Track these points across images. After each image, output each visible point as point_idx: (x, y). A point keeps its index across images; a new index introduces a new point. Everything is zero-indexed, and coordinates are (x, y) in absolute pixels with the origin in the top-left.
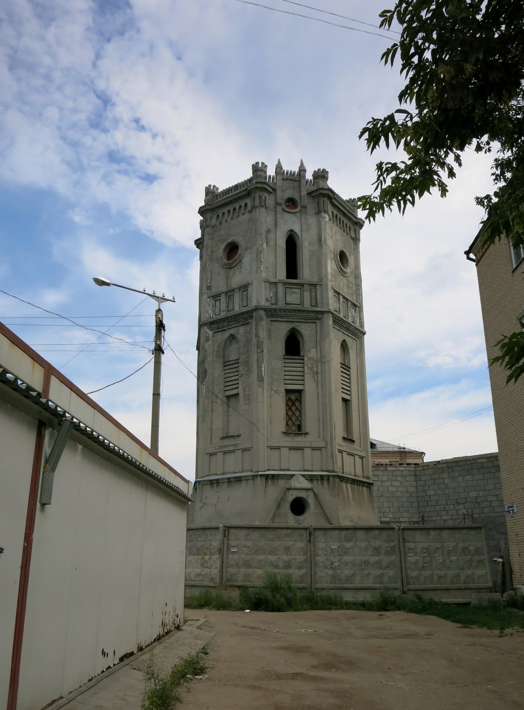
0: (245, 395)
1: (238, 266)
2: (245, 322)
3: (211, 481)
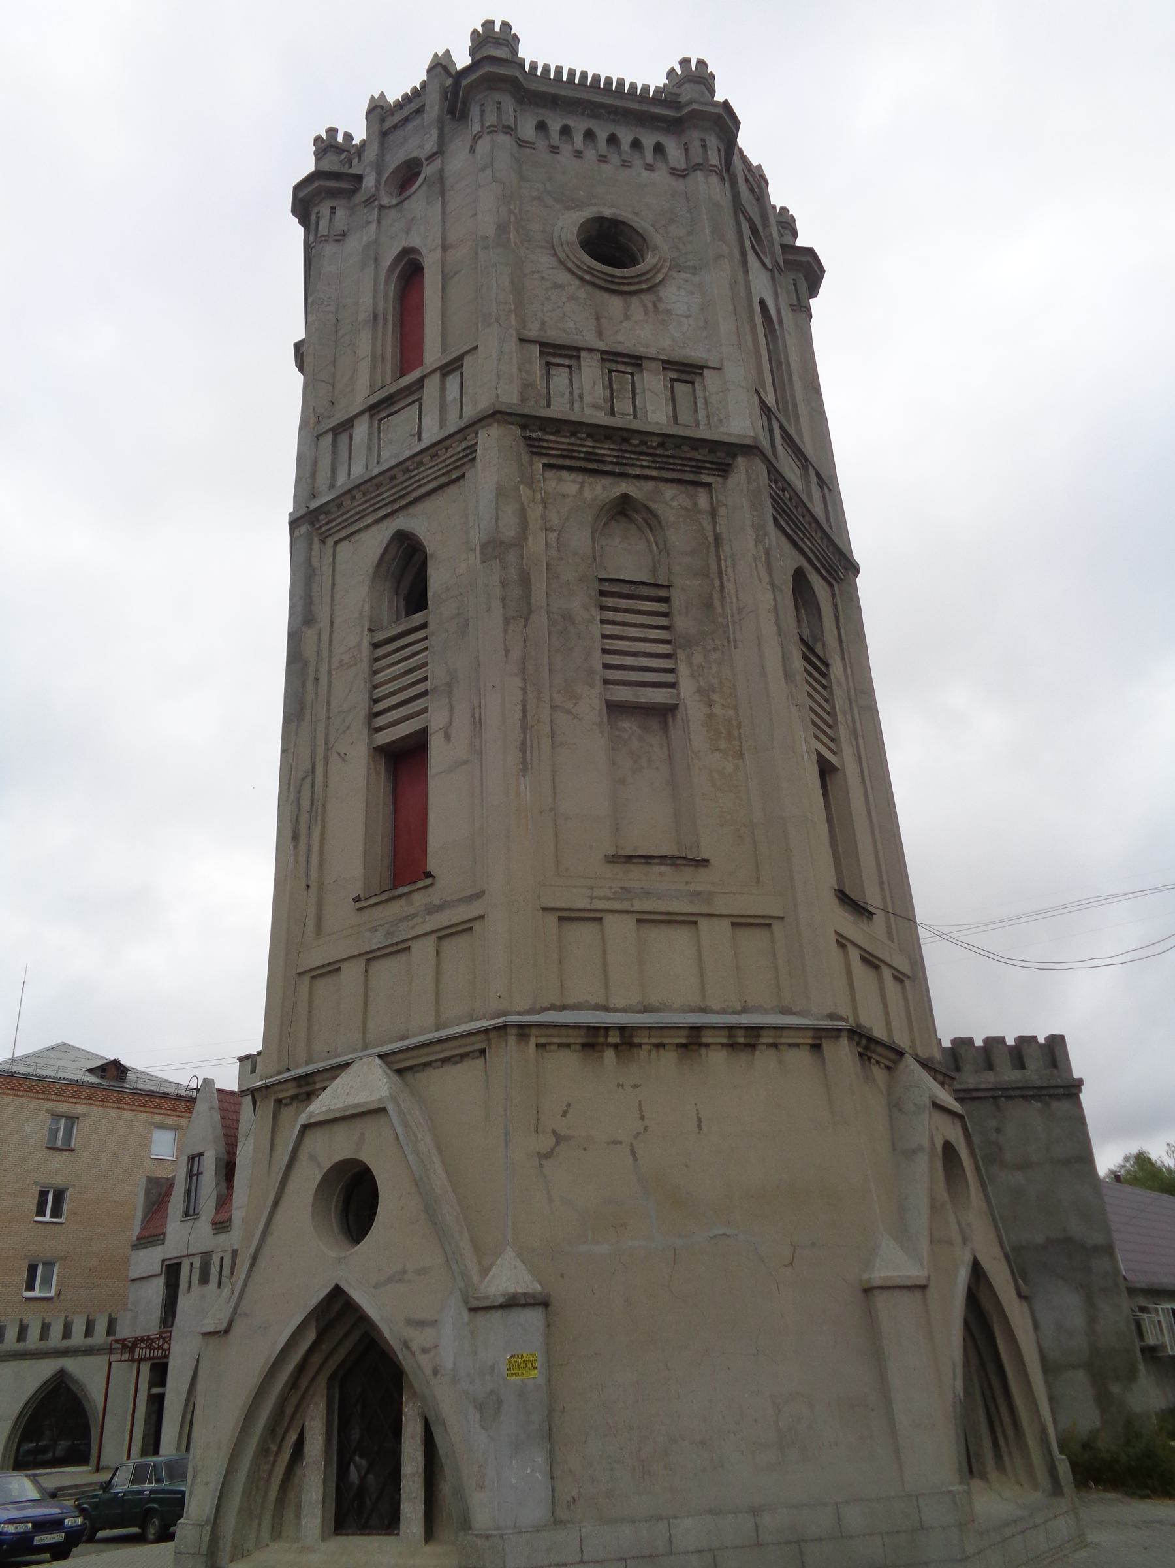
0: (711, 716)
1: (647, 298)
2: (690, 477)
3: (594, 1029)
